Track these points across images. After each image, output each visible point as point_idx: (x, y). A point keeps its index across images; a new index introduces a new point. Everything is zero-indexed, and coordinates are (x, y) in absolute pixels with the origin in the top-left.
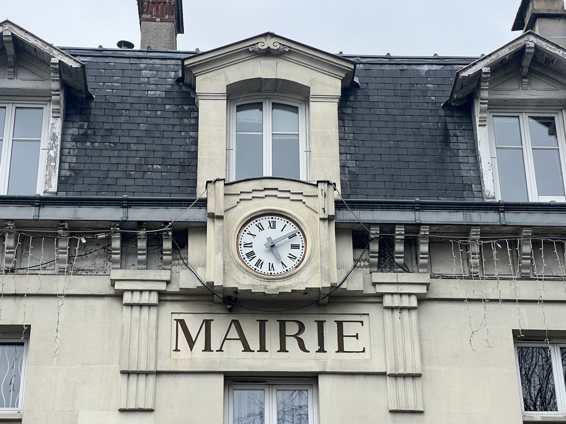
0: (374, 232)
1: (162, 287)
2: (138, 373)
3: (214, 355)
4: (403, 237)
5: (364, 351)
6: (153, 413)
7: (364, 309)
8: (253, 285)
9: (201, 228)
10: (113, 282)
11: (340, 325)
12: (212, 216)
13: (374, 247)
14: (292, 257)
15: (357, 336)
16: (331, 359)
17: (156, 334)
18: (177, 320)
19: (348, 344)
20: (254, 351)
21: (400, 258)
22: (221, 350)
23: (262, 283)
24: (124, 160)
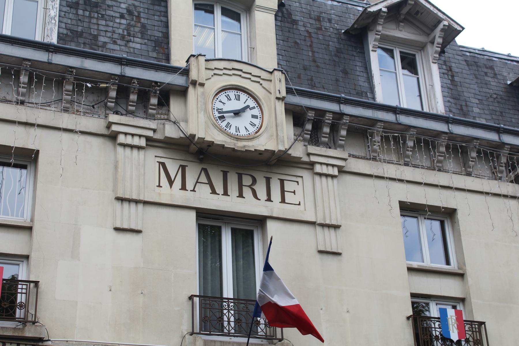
0: (311, 115)
1: (150, 134)
2: (129, 201)
3: (188, 194)
4: (330, 122)
5: (299, 204)
6: (140, 236)
7: (300, 172)
8: (225, 142)
9: (183, 92)
10: (109, 125)
11: (282, 182)
12: (194, 83)
13: (309, 127)
14: (253, 125)
15: (294, 192)
16: (275, 208)
17: (143, 171)
18: (160, 163)
19: (289, 197)
20: (219, 194)
21: (326, 137)
22: (194, 190)
23: (232, 141)
24: (110, 29)
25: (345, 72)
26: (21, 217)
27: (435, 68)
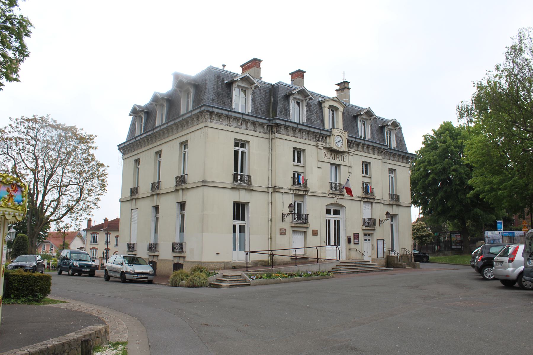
9: (329, 136)
27: (370, 126)
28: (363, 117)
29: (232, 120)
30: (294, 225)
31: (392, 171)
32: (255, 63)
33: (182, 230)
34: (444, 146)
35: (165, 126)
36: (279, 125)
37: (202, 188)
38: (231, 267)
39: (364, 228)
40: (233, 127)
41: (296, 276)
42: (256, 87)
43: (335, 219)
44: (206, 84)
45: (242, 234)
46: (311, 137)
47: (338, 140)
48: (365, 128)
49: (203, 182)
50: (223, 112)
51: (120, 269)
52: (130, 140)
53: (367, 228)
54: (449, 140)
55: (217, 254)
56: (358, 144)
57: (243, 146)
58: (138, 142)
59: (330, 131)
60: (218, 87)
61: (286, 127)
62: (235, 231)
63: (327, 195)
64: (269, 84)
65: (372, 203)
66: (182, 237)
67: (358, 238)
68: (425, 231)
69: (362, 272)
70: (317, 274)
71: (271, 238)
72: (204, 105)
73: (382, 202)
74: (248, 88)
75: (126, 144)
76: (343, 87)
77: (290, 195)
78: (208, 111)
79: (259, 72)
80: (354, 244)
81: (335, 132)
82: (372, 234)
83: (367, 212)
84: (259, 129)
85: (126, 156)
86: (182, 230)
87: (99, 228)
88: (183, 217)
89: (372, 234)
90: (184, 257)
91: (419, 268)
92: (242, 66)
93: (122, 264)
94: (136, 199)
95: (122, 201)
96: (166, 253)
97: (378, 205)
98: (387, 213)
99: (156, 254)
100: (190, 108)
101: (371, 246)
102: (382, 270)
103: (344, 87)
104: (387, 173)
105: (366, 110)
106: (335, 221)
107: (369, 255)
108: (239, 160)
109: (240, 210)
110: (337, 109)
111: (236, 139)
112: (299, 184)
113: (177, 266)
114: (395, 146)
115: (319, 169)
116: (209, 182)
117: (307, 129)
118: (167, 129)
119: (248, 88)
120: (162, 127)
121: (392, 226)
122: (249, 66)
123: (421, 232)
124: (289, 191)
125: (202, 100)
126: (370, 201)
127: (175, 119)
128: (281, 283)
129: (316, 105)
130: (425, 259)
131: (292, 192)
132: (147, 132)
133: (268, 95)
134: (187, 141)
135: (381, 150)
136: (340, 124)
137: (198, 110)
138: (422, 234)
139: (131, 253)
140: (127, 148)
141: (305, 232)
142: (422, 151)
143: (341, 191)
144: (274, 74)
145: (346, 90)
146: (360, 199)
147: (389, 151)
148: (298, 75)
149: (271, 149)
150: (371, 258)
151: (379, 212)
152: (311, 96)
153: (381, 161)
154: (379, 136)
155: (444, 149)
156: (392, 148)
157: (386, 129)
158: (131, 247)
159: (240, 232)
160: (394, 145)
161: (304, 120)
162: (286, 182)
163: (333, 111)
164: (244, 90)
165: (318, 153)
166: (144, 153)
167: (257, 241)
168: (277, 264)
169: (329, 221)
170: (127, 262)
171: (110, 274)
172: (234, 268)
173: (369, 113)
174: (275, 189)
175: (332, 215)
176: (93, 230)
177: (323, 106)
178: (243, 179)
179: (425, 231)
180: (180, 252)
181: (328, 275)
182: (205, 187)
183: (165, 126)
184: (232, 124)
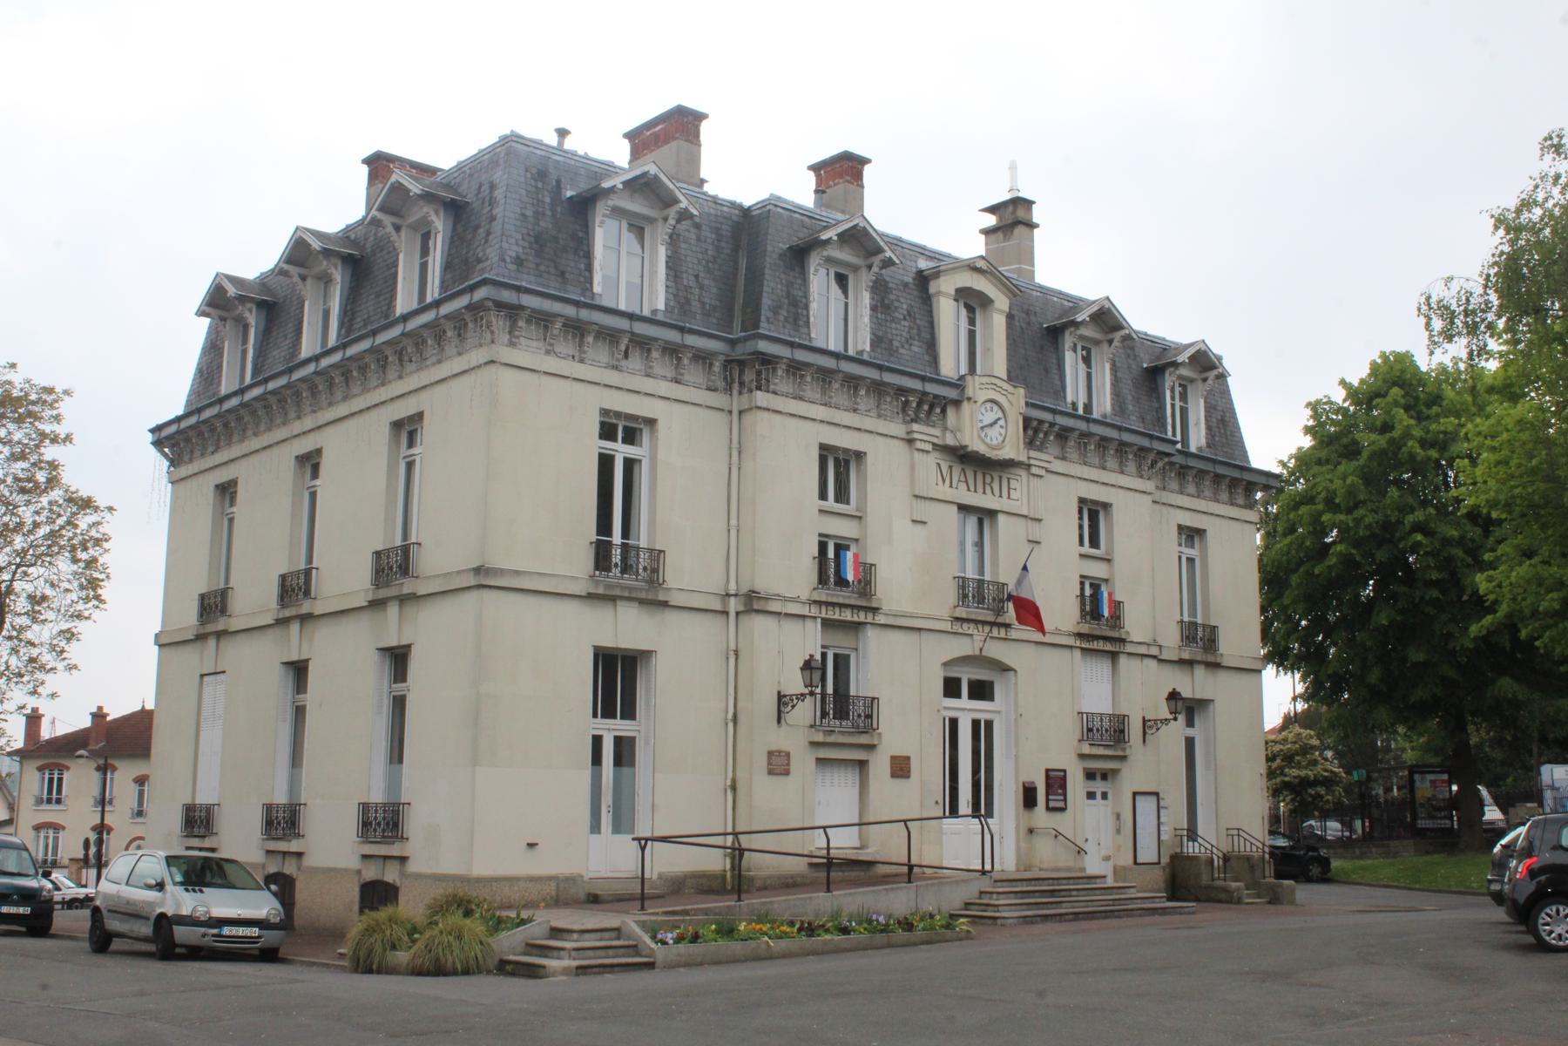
9: (957, 403)
12: (969, 399)
25: (1047, 371)
26: (837, 501)
27: (1107, 366)
28: (1084, 331)
29: (590, 339)
30: (820, 738)
31: (1191, 535)
32: (680, 126)
33: (397, 753)
34: (1382, 441)
35: (336, 358)
36: (767, 361)
37: (474, 595)
38: (582, 896)
39: (1086, 749)
40: (595, 365)
41: (827, 931)
42: (684, 215)
43: (977, 716)
44: (492, 202)
45: (625, 770)
46: (890, 404)
47: (990, 421)
48: (1089, 375)
49: (478, 570)
50: (557, 307)
51: (152, 904)
52: (199, 411)
53: (1095, 751)
54: (1403, 419)
55: (531, 845)
56: (1063, 435)
57: (631, 437)
58: (232, 417)
59: (959, 385)
60: (538, 215)
61: (795, 368)
62: (597, 759)
63: (947, 626)
64: (733, 205)
65: (1114, 656)
66: (394, 782)
67: (1064, 787)
68: (1314, 763)
69: (1076, 916)
70: (907, 925)
71: (734, 788)
72: (484, 282)
73: (1154, 651)
74: (651, 221)
75: (184, 424)
76: (1009, 219)
77: (809, 623)
78: (500, 305)
79: (694, 160)
80: (1048, 809)
81: (974, 387)
82: (1115, 772)
83: (1095, 688)
84: (693, 373)
85: (184, 471)
86: (397, 753)
87: (71, 745)
88: (399, 704)
89: (1115, 772)
90: (403, 859)
91: (1292, 902)
92: (631, 136)
93: (160, 886)
94: (220, 635)
95: (165, 643)
96: (331, 844)
97: (1136, 662)
98: (1173, 696)
99: (294, 846)
100: (433, 292)
101: (1111, 820)
102: (1153, 911)
103: (1013, 218)
104: (1171, 544)
105: (1095, 308)
106: (976, 724)
107: (1104, 853)
108: (615, 491)
109: (617, 679)
110: (986, 302)
111: (605, 412)
112: (841, 582)
113: (377, 894)
114: (1203, 442)
115: (920, 526)
116: (501, 572)
117: (873, 374)
118: (344, 368)
119: (651, 221)
120: (325, 362)
121: (1190, 742)
122: (656, 136)
123: (1299, 766)
124: (805, 611)
125: (479, 261)
126: (1108, 647)
127: (374, 333)
128: (770, 957)
129: (906, 285)
130: (1315, 870)
131: (814, 611)
132: (266, 381)
133: (727, 248)
134: (420, 415)
135: (1151, 456)
136: (996, 357)
137: (463, 301)
138: (1303, 773)
139: (195, 842)
140: (187, 440)
141: (862, 764)
142: (1303, 459)
143: (999, 611)
144: (751, 166)
145: (1020, 230)
146: (1070, 641)
147: (1178, 459)
148: (842, 171)
149: (738, 450)
150: (1110, 864)
151: (1141, 689)
152: (889, 254)
153: (1148, 499)
154: (1140, 403)
155: (1383, 452)
156: (1193, 449)
157: (1169, 380)
158: (198, 820)
159: (619, 761)
160: (1198, 439)
161: (861, 341)
162: (792, 575)
163: (970, 309)
164: (638, 228)
165: (912, 467)
166: (255, 459)
167: (685, 799)
168: (758, 884)
169: (954, 723)
170: (179, 878)
171: (113, 924)
172: (594, 900)
173: (1106, 319)
174: (753, 602)
175: (964, 702)
176: (49, 754)
177: (932, 289)
178: (632, 561)
179: (1314, 763)
180: (385, 840)
181: (948, 926)
182: (486, 593)
183: (336, 358)
184: (590, 353)
